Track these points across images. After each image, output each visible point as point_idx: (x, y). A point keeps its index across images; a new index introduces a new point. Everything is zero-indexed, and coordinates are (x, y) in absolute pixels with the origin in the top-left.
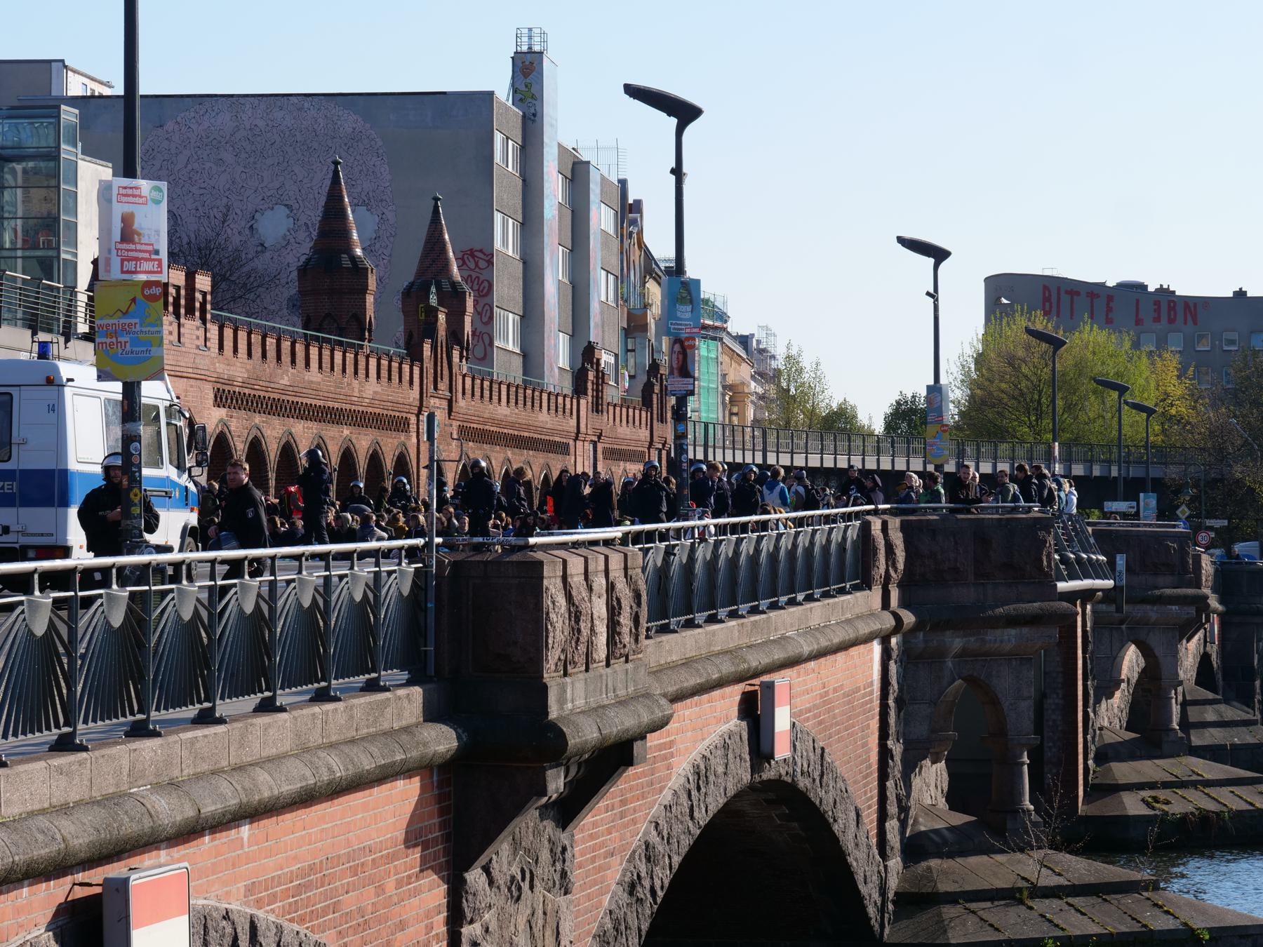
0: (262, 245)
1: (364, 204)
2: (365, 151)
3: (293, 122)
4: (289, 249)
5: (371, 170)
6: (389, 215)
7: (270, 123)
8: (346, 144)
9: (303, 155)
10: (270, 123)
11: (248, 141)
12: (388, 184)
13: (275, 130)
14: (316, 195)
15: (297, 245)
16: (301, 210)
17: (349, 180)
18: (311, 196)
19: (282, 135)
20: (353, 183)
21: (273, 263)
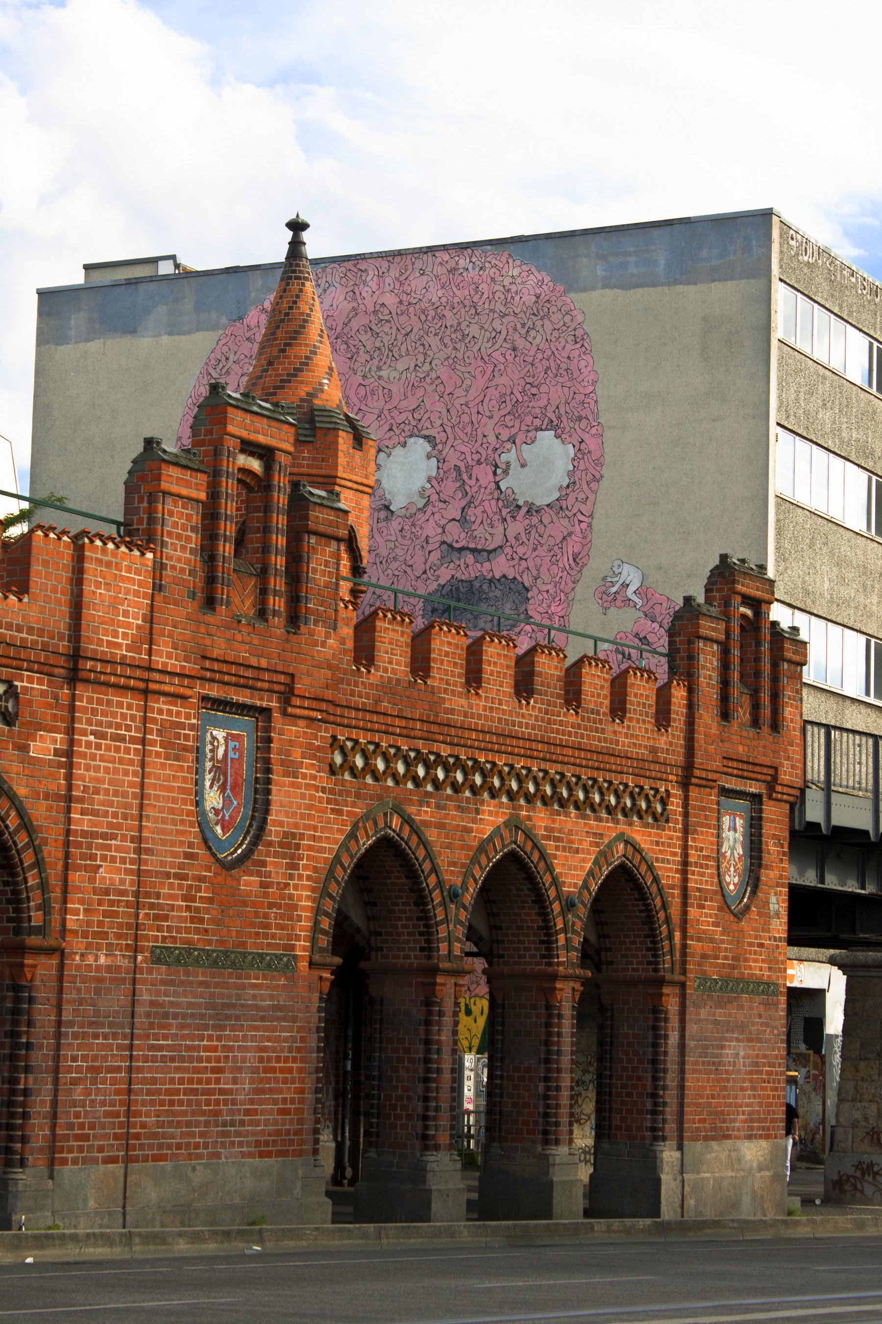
0: (387, 508)
1: (551, 426)
2: (556, 334)
3: (440, 294)
4: (429, 512)
5: (564, 366)
6: (591, 443)
7: (404, 297)
8: (523, 325)
9: (455, 348)
10: (404, 297)
11: (369, 333)
12: (591, 388)
13: (411, 309)
14: (475, 417)
15: (442, 505)
16: (449, 444)
17: (528, 386)
18: (465, 418)
19: (423, 318)
20: (534, 391)
21: (404, 537)
